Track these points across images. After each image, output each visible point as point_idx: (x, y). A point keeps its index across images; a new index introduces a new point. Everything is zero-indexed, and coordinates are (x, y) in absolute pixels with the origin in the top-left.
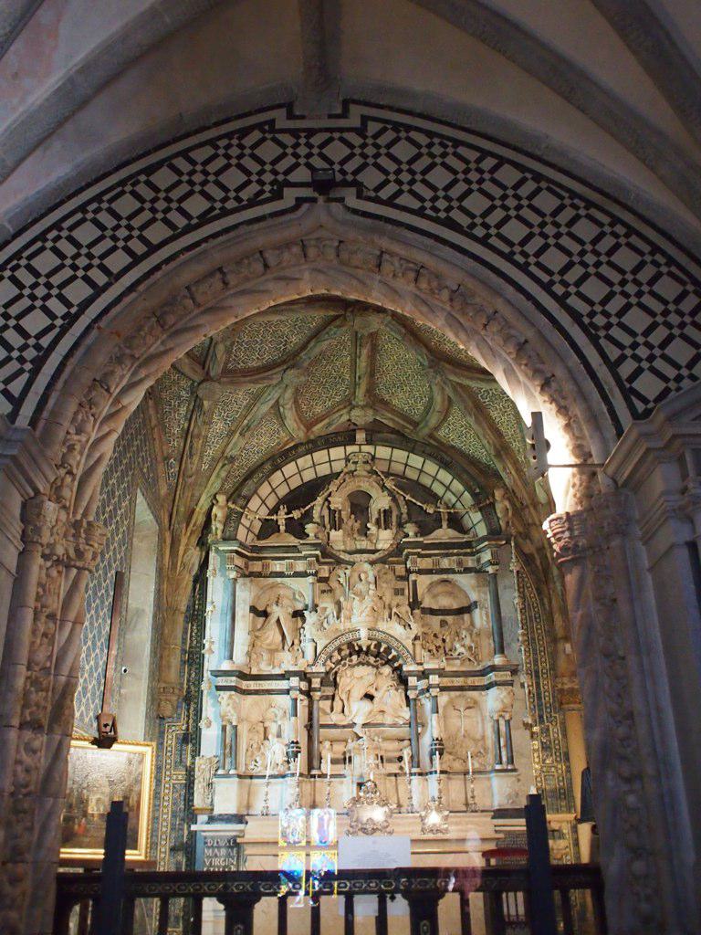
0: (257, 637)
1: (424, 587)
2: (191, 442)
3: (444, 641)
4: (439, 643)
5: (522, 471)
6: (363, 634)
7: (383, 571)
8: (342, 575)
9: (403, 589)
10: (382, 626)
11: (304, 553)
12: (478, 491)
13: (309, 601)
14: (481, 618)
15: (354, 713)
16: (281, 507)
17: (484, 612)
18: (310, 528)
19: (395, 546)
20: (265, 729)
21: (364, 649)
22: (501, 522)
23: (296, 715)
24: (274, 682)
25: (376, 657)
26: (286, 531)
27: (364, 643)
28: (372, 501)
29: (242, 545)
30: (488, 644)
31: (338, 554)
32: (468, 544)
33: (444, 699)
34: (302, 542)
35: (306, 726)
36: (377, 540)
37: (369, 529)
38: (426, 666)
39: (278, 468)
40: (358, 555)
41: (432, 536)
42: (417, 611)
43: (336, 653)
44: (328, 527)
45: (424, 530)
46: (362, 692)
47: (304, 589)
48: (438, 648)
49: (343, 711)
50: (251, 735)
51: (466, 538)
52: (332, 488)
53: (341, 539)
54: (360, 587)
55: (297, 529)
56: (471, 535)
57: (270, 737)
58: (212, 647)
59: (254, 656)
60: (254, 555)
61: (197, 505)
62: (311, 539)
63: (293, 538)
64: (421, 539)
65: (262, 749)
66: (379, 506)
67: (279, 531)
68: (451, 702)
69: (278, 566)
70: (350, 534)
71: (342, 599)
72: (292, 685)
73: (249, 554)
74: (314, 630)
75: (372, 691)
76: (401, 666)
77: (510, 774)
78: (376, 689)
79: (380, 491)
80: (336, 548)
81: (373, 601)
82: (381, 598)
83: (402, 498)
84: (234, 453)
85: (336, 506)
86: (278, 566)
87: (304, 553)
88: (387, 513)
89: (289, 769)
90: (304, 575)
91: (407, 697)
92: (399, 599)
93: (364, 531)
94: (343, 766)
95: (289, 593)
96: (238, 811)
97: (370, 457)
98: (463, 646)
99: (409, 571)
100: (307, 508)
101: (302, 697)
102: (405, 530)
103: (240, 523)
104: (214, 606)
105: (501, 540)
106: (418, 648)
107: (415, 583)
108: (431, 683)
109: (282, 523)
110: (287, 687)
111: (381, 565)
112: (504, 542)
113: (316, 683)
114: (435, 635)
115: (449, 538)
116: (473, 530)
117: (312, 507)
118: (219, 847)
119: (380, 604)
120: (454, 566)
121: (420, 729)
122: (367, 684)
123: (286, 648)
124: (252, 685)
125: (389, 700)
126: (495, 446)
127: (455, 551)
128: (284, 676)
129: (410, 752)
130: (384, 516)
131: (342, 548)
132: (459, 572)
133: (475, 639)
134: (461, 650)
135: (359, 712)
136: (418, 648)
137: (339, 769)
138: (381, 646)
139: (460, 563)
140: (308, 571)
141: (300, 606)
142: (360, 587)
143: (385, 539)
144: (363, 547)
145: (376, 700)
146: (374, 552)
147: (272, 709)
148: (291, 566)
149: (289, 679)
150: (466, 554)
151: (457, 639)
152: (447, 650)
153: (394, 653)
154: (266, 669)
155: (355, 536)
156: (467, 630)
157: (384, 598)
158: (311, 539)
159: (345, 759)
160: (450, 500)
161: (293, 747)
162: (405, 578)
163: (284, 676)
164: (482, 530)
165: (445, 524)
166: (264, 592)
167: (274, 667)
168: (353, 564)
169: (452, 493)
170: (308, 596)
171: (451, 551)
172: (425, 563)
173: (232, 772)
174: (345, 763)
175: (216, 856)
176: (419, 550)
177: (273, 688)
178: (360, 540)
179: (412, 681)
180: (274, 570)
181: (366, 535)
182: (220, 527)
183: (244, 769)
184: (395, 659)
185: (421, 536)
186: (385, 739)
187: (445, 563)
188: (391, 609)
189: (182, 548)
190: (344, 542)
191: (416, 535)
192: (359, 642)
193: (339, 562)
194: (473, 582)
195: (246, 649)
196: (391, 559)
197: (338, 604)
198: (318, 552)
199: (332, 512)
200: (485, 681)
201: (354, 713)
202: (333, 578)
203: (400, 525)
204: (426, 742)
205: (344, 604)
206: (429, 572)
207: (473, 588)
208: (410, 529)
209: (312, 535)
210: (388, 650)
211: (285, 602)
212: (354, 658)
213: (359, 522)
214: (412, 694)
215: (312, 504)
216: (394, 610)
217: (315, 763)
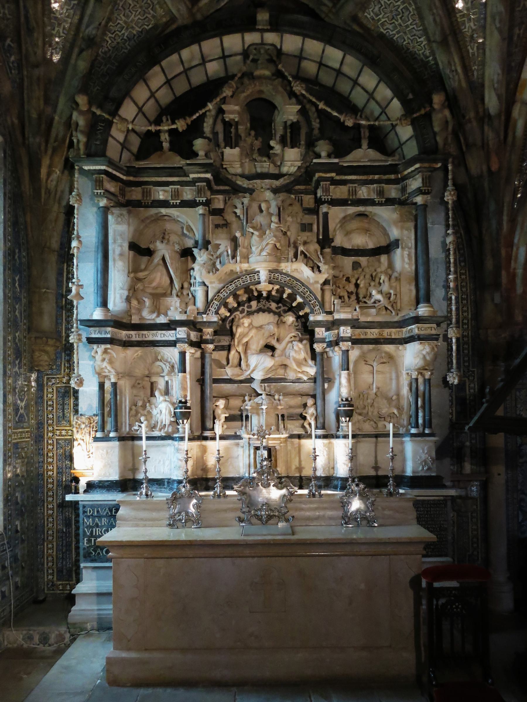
0: (139, 280)
1: (338, 220)
2: (25, 7)
3: (357, 286)
4: (351, 288)
5: (471, 69)
6: (263, 276)
7: (289, 202)
8: (239, 206)
9: (311, 225)
10: (287, 267)
11: (192, 176)
12: (411, 96)
13: (198, 236)
14: (403, 260)
15: (251, 368)
16: (164, 119)
17: (406, 253)
18: (199, 144)
19: (303, 170)
20: (152, 384)
21: (265, 294)
22: (438, 138)
23: (184, 371)
24: (160, 332)
25: (278, 304)
26: (170, 150)
27: (264, 287)
28: (276, 112)
29: (111, 163)
30: (408, 291)
31: (234, 179)
32: (393, 169)
33: (354, 354)
34: (188, 162)
35: (198, 381)
36: (282, 160)
37: (272, 148)
38: (337, 316)
39: (155, 61)
40: (258, 181)
41: (349, 157)
42: (328, 250)
43: (230, 300)
44: (223, 145)
45: (339, 151)
46: (262, 343)
47: (193, 220)
48: (350, 294)
49: (240, 365)
50: (135, 392)
51: (390, 161)
52: (227, 92)
53: (237, 158)
54: (260, 219)
55: (182, 145)
56: (397, 157)
57: (157, 393)
58: (82, 292)
59: (134, 303)
60: (131, 178)
61: (55, 112)
62: (201, 159)
63: (178, 158)
64: (336, 161)
65: (148, 408)
66: (285, 117)
67: (160, 148)
68: (363, 358)
69: (161, 194)
70: (248, 154)
71: (238, 234)
72: (178, 336)
73: (124, 178)
74: (204, 272)
75: (274, 343)
76: (306, 315)
77: (427, 438)
78: (278, 340)
79: (287, 98)
80: (231, 170)
81: (275, 236)
82: (285, 234)
83: (314, 109)
84: (91, 31)
85: (232, 116)
86: (161, 193)
87: (192, 176)
88: (294, 127)
89: (178, 431)
90: (191, 204)
91: (313, 350)
92: (305, 236)
93: (266, 151)
94: (239, 423)
95: (176, 228)
96: (122, 473)
97: (275, 53)
98: (381, 292)
99: (319, 202)
100: (194, 117)
101: (193, 350)
102: (317, 149)
103: (109, 135)
104: (80, 242)
105: (436, 161)
106: (328, 294)
107: (326, 215)
108: (342, 335)
109: (165, 137)
110: (174, 339)
111: (285, 194)
112: (439, 165)
113: (208, 332)
114: (348, 280)
115: (370, 161)
116: (400, 149)
117: (202, 117)
118: (100, 517)
119: (284, 241)
120: (373, 196)
121: (326, 385)
122: (267, 334)
123: (174, 292)
124: (134, 336)
125: (292, 354)
126: (442, 29)
127: (376, 177)
128: (171, 325)
129: (315, 412)
130: (291, 133)
131: (239, 171)
132: (380, 204)
133: (394, 284)
134: (379, 297)
135: (259, 366)
136: (328, 295)
137: (235, 427)
138: (283, 292)
139: (381, 193)
140: (197, 199)
141: (190, 243)
142: (260, 219)
143: (292, 160)
144: (265, 170)
145: (277, 353)
146: (277, 177)
147: (158, 363)
148: (176, 194)
149: (175, 329)
150: (389, 182)
151: (373, 284)
152: (361, 296)
153: (299, 299)
154: (149, 317)
155: (254, 157)
156: (386, 273)
157: (289, 233)
158: (201, 159)
159: (241, 416)
160: (372, 113)
161: (181, 408)
162: (314, 211)
163: (171, 325)
164: (411, 150)
165: (365, 144)
166: (146, 226)
167: (158, 316)
168: (251, 191)
169: (377, 102)
170: (198, 231)
171: (371, 177)
172: (340, 192)
173: (112, 435)
174: (242, 420)
175: (97, 526)
176: (333, 175)
177: (159, 338)
178: (261, 162)
179: (320, 332)
180: (157, 198)
181: (269, 156)
182: (83, 139)
183: (128, 429)
184: (301, 306)
185: (335, 158)
186: (286, 395)
187: (363, 192)
188: (296, 248)
189: (44, 171)
190: (242, 165)
191: (329, 156)
192: (259, 287)
193: (237, 190)
194: (395, 216)
195: (126, 293)
196: (297, 187)
197: (234, 240)
198: (209, 176)
199: (227, 125)
200: (405, 332)
201: (251, 368)
202: (229, 210)
203: (310, 145)
204: (333, 397)
205: (241, 240)
206: (342, 203)
207: (395, 223)
208: (323, 148)
209: (201, 153)
210: (292, 297)
211: (174, 238)
212: (254, 303)
213: (260, 139)
214: (318, 347)
215: (201, 112)
216: (301, 248)
217: (209, 424)
